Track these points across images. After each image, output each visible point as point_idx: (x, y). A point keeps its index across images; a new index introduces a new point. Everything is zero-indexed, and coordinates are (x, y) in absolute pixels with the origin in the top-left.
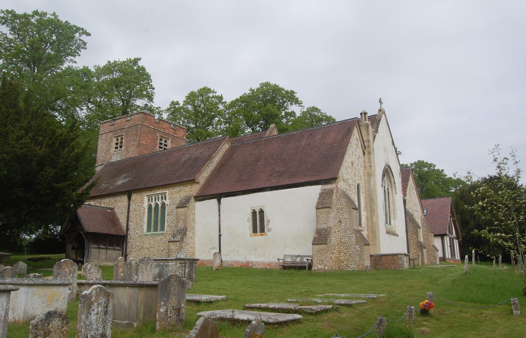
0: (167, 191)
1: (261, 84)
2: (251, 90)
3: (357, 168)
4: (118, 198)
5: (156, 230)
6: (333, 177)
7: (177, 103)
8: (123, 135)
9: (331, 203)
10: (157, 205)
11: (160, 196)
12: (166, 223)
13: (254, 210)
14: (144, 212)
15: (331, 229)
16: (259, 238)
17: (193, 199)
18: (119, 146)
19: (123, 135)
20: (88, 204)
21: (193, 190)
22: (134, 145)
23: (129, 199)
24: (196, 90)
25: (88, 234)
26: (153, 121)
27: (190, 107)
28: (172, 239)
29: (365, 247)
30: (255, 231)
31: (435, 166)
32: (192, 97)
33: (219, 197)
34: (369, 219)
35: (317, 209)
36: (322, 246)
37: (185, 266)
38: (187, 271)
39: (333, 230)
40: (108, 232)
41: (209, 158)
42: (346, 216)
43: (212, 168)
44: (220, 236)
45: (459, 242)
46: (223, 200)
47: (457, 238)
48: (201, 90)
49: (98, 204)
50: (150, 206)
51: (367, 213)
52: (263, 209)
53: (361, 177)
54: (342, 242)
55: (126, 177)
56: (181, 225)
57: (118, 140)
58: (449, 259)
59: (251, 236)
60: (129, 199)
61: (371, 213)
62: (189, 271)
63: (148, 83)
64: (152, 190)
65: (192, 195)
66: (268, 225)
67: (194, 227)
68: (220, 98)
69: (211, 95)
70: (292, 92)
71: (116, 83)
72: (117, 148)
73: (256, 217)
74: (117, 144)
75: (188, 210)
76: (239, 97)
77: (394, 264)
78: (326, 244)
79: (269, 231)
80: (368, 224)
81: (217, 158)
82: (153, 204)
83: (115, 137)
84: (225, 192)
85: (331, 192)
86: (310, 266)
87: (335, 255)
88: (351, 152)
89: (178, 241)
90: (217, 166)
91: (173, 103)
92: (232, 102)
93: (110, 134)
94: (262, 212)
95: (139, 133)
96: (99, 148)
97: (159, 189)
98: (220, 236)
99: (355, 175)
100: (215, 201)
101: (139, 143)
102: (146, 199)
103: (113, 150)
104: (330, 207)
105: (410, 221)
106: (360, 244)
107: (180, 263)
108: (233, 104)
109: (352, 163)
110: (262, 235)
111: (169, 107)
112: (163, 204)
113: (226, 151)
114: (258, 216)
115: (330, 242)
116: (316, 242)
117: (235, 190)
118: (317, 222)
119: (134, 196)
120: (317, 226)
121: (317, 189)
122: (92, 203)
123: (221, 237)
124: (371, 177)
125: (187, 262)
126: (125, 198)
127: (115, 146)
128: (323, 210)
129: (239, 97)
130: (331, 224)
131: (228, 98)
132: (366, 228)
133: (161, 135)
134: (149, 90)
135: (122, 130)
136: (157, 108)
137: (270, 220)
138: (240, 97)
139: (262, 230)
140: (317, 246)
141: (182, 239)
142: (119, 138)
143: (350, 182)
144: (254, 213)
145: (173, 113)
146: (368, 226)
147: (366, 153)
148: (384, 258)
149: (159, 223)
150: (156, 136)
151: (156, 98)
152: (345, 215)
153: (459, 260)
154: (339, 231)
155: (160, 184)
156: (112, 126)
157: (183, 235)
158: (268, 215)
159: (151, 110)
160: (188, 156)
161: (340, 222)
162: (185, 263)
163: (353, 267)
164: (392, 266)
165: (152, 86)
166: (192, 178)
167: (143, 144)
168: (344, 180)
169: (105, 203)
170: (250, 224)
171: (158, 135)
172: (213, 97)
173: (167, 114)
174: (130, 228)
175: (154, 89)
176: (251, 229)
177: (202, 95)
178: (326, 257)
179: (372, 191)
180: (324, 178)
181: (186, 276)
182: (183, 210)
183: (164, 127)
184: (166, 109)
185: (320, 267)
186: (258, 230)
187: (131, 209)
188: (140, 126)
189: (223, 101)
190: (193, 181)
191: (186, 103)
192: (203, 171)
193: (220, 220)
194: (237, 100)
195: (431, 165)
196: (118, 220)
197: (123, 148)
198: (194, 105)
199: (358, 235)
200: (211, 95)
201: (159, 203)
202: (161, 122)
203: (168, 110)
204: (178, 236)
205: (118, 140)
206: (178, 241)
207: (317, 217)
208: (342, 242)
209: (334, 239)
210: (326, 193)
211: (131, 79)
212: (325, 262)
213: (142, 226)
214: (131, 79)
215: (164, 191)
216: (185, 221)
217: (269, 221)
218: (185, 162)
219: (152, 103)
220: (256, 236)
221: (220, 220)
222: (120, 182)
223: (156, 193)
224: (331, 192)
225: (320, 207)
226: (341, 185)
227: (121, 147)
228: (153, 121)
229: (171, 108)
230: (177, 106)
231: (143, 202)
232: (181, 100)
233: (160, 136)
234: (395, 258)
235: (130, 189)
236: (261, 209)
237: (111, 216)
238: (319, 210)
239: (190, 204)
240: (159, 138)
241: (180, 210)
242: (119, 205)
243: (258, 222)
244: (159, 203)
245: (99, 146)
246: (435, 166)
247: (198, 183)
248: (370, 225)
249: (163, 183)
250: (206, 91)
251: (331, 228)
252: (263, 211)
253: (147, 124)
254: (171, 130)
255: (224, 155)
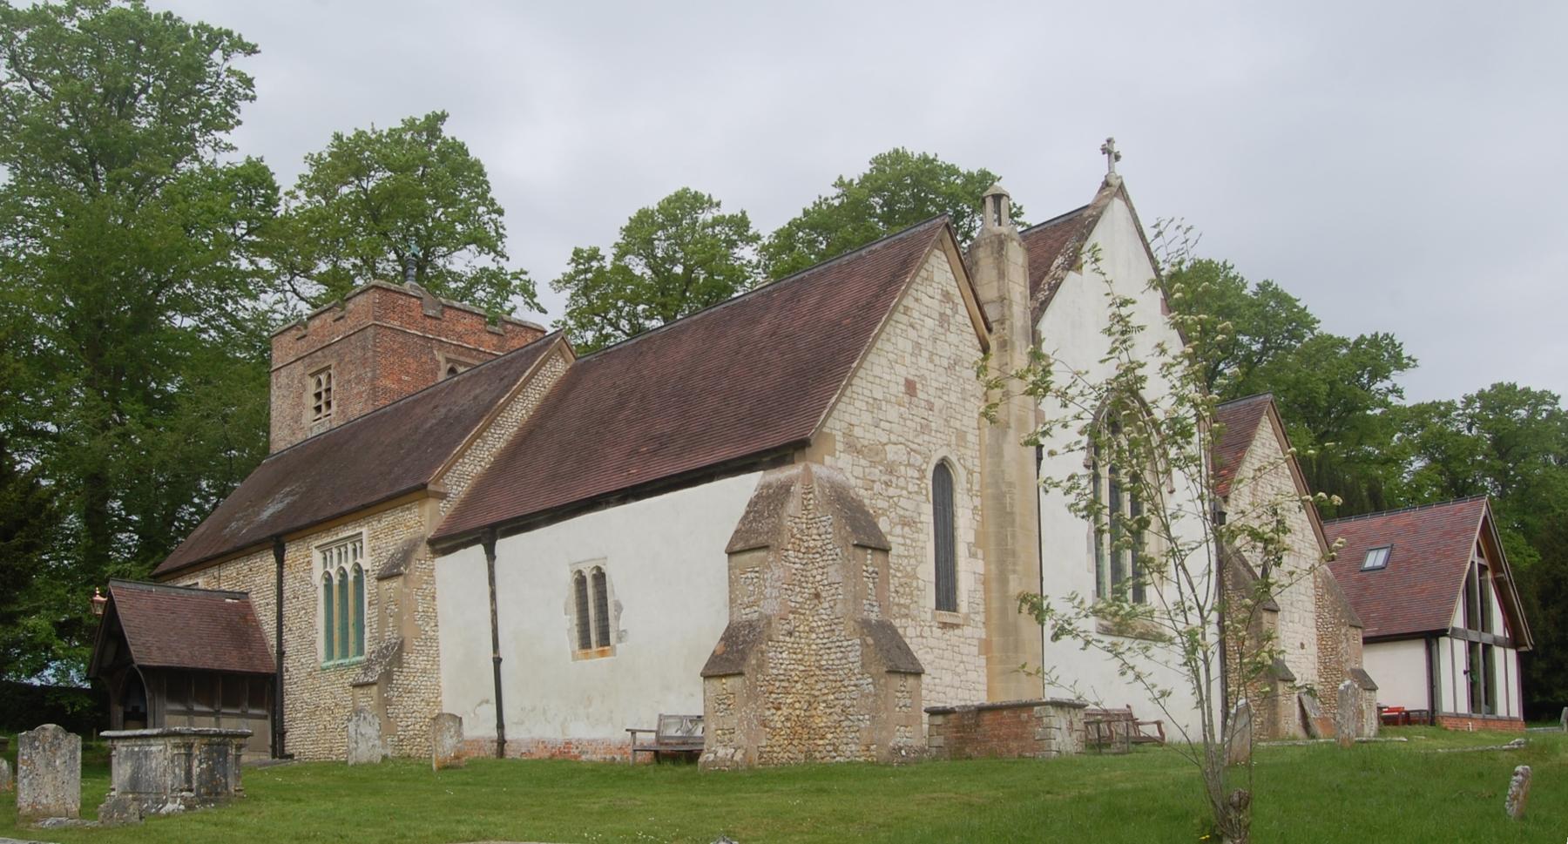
0: (365, 530)
1: (875, 160)
2: (840, 183)
3: (938, 403)
4: (256, 562)
5: (345, 654)
6: (795, 437)
7: (594, 255)
8: (329, 367)
9: (777, 531)
10: (344, 575)
11: (350, 547)
12: (367, 630)
13: (580, 572)
14: (316, 600)
15: (769, 623)
16: (596, 665)
17: (423, 550)
18: (323, 401)
19: (329, 367)
20: (188, 588)
21: (422, 520)
22: (360, 394)
23: (280, 561)
24: (653, 204)
25: (151, 671)
26: (417, 313)
27: (639, 267)
28: (363, 679)
29: (897, 681)
30: (585, 643)
31: (1556, 399)
32: (640, 232)
33: (488, 536)
34: (994, 586)
35: (731, 553)
36: (729, 683)
37: (189, 756)
38: (196, 770)
39: (780, 628)
40: (216, 666)
41: (487, 412)
42: (834, 574)
43: (501, 445)
44: (497, 662)
45: (1520, 656)
46: (503, 546)
47: (1514, 641)
48: (669, 200)
49: (214, 586)
50: (328, 578)
51: (987, 564)
52: (606, 569)
53: (961, 436)
54: (820, 667)
55: (287, 495)
56: (390, 635)
57: (319, 383)
58: (1457, 716)
59: (575, 658)
60: (280, 561)
61: (1001, 563)
62: (211, 770)
63: (483, 198)
64: (329, 530)
65: (422, 537)
66: (617, 618)
67: (434, 639)
68: (740, 224)
69: (706, 216)
70: (985, 178)
71: (374, 209)
72: (318, 409)
73: (586, 596)
74: (318, 396)
75: (406, 583)
76: (799, 214)
77: (1017, 737)
78: (741, 674)
79: (620, 639)
80: (987, 601)
81: (519, 412)
82: (333, 572)
83: (312, 375)
84: (506, 517)
85: (784, 490)
86: (692, 757)
87: (785, 711)
88: (905, 345)
89: (374, 684)
90: (517, 436)
91: (577, 253)
92: (778, 234)
93: (299, 368)
94: (600, 577)
95: (370, 354)
96: (274, 414)
97: (345, 524)
98: (497, 662)
99: (925, 428)
100: (479, 550)
101: (374, 388)
102: (317, 557)
103: (309, 414)
104: (765, 547)
105: (1236, 586)
106: (873, 670)
107: (176, 746)
108: (786, 238)
109: (910, 387)
110: (603, 654)
111: (570, 269)
112: (358, 570)
113: (557, 385)
114: (590, 591)
115: (761, 666)
116: (717, 668)
117: (529, 511)
118: (732, 601)
119: (292, 552)
120: (731, 614)
121: (746, 486)
122: (201, 581)
123: (503, 666)
124: (1005, 433)
125: (197, 742)
126: (270, 560)
127: (313, 402)
128: (747, 557)
129: (799, 214)
130: (770, 607)
131: (766, 225)
132: (980, 618)
133: (452, 356)
134: (486, 218)
135: (326, 351)
136: (515, 276)
137: (623, 603)
138: (806, 213)
139: (604, 639)
140: (716, 683)
141: (387, 677)
142: (323, 377)
143: (893, 453)
144: (581, 582)
145: (586, 289)
146: (987, 611)
147: (993, 345)
148: (987, 717)
149: (351, 630)
150: (433, 359)
151: (508, 246)
152: (831, 570)
153: (1511, 720)
154: (812, 630)
155: (345, 508)
156: (303, 342)
157: (390, 664)
158: (617, 589)
159: (499, 283)
160: (443, 411)
161: (817, 596)
162: (191, 746)
163: (851, 751)
164: (1013, 745)
165: (492, 202)
166: (422, 481)
167: (386, 390)
168: (853, 447)
169: (229, 578)
170: (570, 621)
171: (440, 357)
172: (717, 222)
173: (567, 293)
174: (288, 650)
175: (500, 212)
176: (575, 634)
177: (676, 221)
178: (741, 721)
179: (1010, 484)
180: (768, 445)
181: (195, 785)
182: (394, 584)
183: (459, 328)
184: (560, 277)
185: (721, 752)
186: (594, 637)
187: (287, 594)
188: (370, 331)
189: (750, 233)
190: (418, 492)
191: (622, 252)
192: (462, 455)
193: (494, 613)
194: (796, 225)
195: (1542, 398)
196: (257, 627)
197: (334, 404)
198: (650, 256)
199: (870, 641)
200: (706, 216)
201: (348, 567)
202: (449, 314)
203: (569, 279)
204: (377, 668)
205: (319, 383)
206: (374, 684)
207: (731, 582)
208: (820, 667)
209: (780, 658)
210: (769, 496)
211: (413, 190)
212: (739, 737)
213: (313, 642)
214: (413, 190)
215: (358, 530)
216: (398, 617)
217: (619, 608)
218: (430, 432)
219: (503, 261)
220: (587, 656)
221: (494, 613)
222: (266, 515)
223: (341, 536)
224: (784, 490)
225: (738, 547)
226: (833, 465)
227: (328, 404)
228: (417, 313)
229: (578, 273)
230: (595, 264)
231: (312, 563)
232: (606, 241)
233: (448, 360)
234: (1024, 716)
235: (280, 529)
236: (599, 569)
237: (237, 619)
238: (736, 559)
239: (414, 564)
240: (445, 367)
241: (386, 585)
242: (253, 578)
243: (594, 611)
244: (348, 567)
245: (273, 406)
246: (1556, 399)
247: (443, 496)
248: (995, 605)
249: (353, 505)
250: (685, 204)
251: (769, 618)
252: (603, 575)
253: (396, 324)
254: (487, 337)
255: (547, 399)
